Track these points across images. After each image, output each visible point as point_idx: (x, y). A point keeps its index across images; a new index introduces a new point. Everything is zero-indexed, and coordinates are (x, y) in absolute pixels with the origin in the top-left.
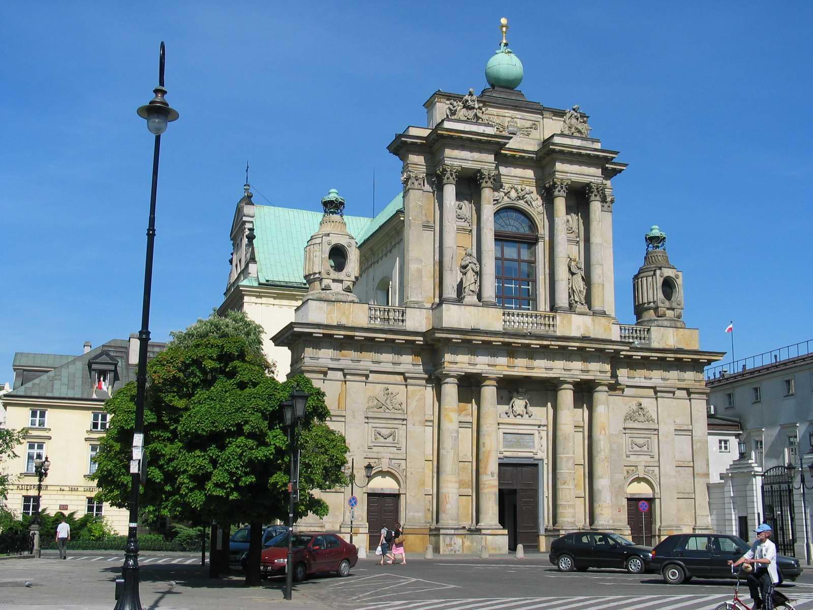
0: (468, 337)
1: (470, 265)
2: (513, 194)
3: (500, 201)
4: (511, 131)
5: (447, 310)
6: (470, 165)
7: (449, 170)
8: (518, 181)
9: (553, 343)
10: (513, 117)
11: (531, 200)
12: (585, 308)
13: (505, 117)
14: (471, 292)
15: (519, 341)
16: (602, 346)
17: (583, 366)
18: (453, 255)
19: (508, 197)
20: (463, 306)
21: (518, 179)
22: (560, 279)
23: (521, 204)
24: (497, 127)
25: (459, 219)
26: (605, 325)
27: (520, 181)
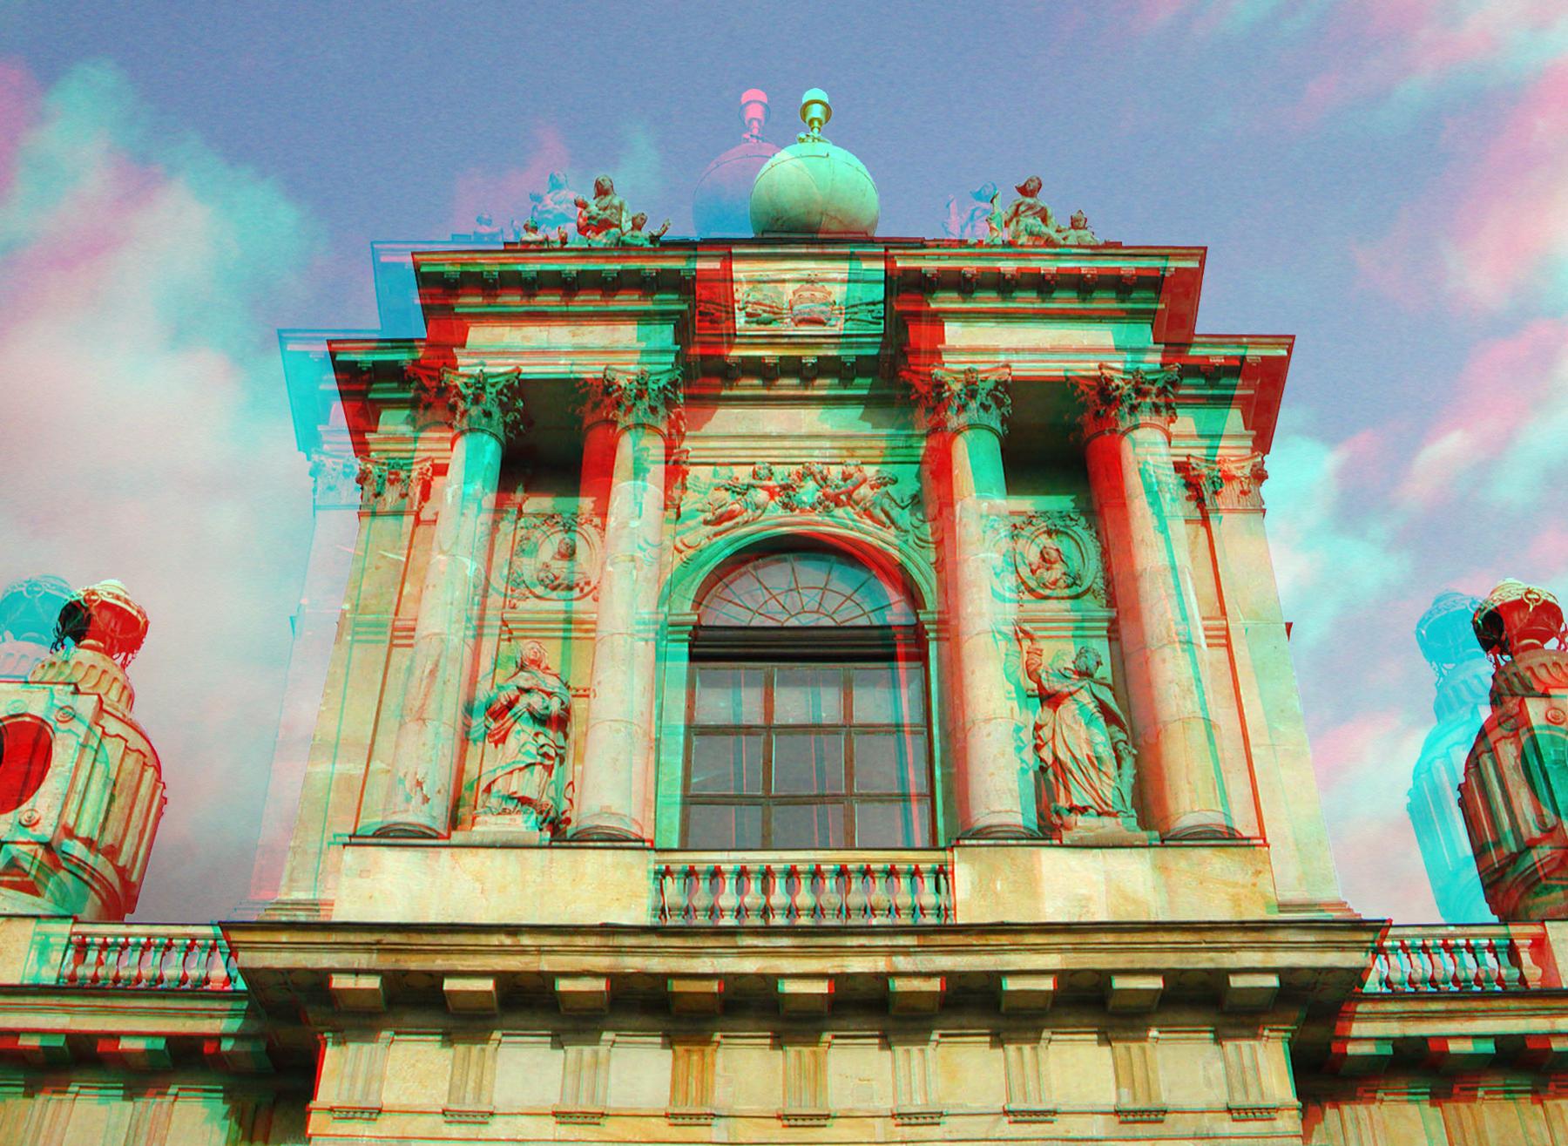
0: (414, 963)
1: (525, 700)
2: (809, 492)
3: (745, 517)
4: (800, 312)
5: (365, 873)
6: (561, 369)
7: (470, 391)
8: (828, 453)
9: (902, 963)
10: (813, 277)
11: (886, 503)
12: (1125, 825)
13: (783, 281)
14: (511, 805)
15: (704, 965)
16: (1204, 961)
17: (1124, 1091)
18: (436, 665)
19: (785, 506)
20: (445, 852)
21: (828, 444)
22: (980, 717)
23: (844, 523)
24: (749, 310)
25: (554, 589)
26: (1235, 885)
27: (836, 452)
